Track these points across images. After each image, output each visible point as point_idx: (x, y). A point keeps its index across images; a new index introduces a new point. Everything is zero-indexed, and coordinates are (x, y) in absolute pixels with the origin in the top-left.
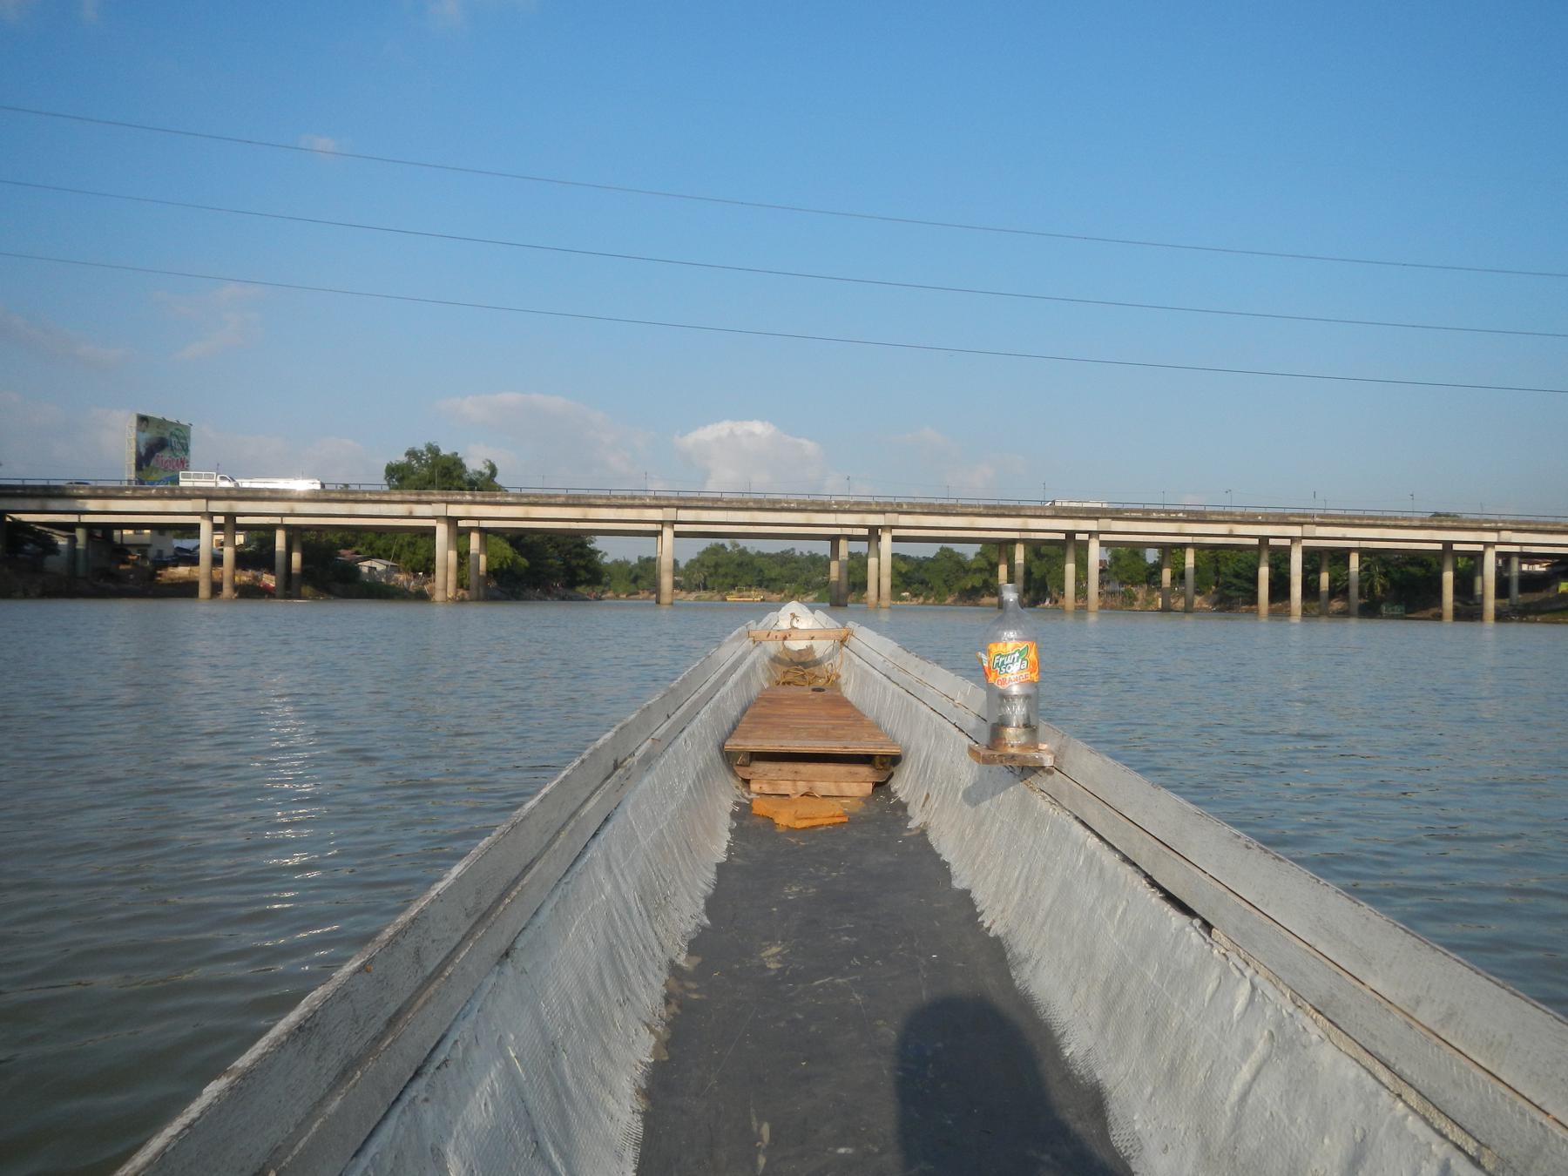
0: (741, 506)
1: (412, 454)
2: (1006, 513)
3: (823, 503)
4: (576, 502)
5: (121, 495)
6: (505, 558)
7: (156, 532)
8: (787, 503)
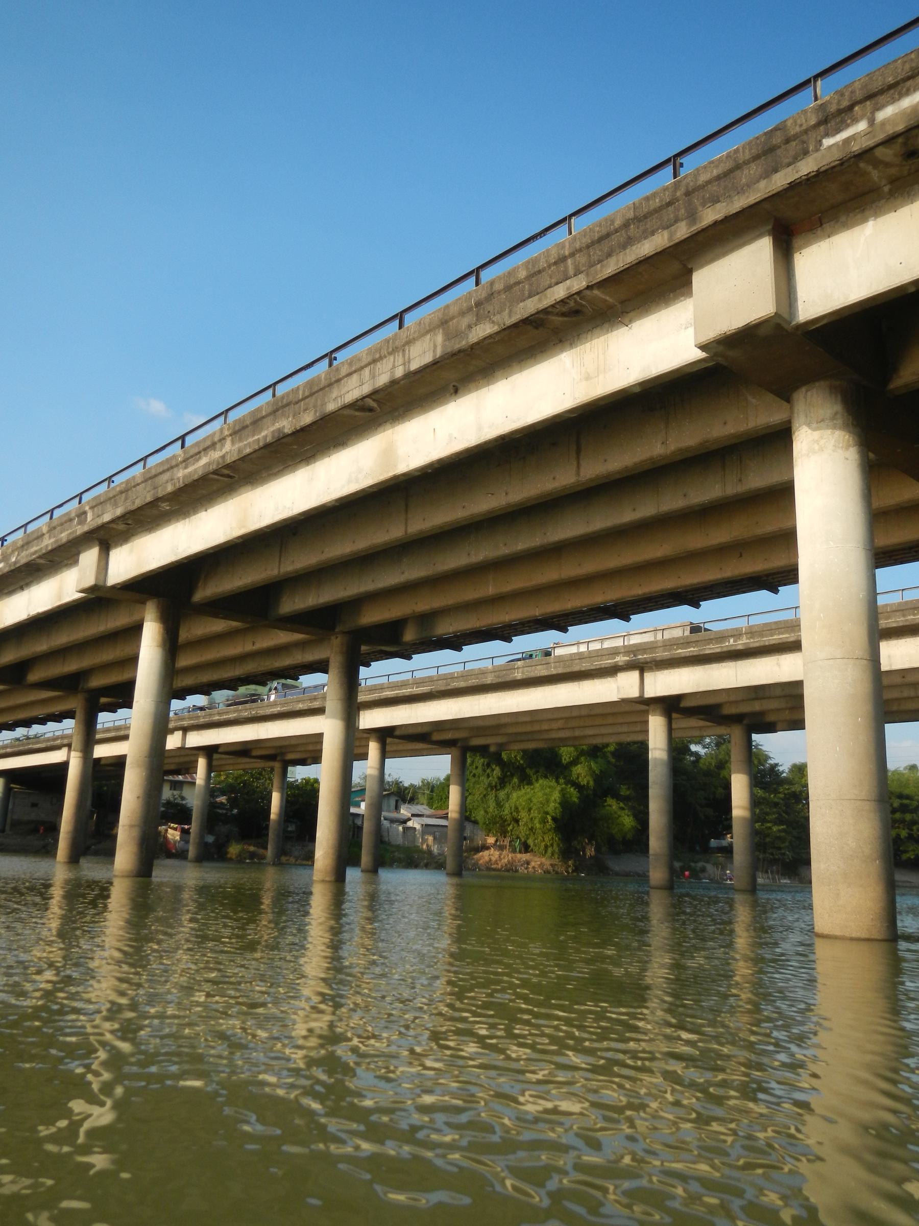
6: (547, 813)
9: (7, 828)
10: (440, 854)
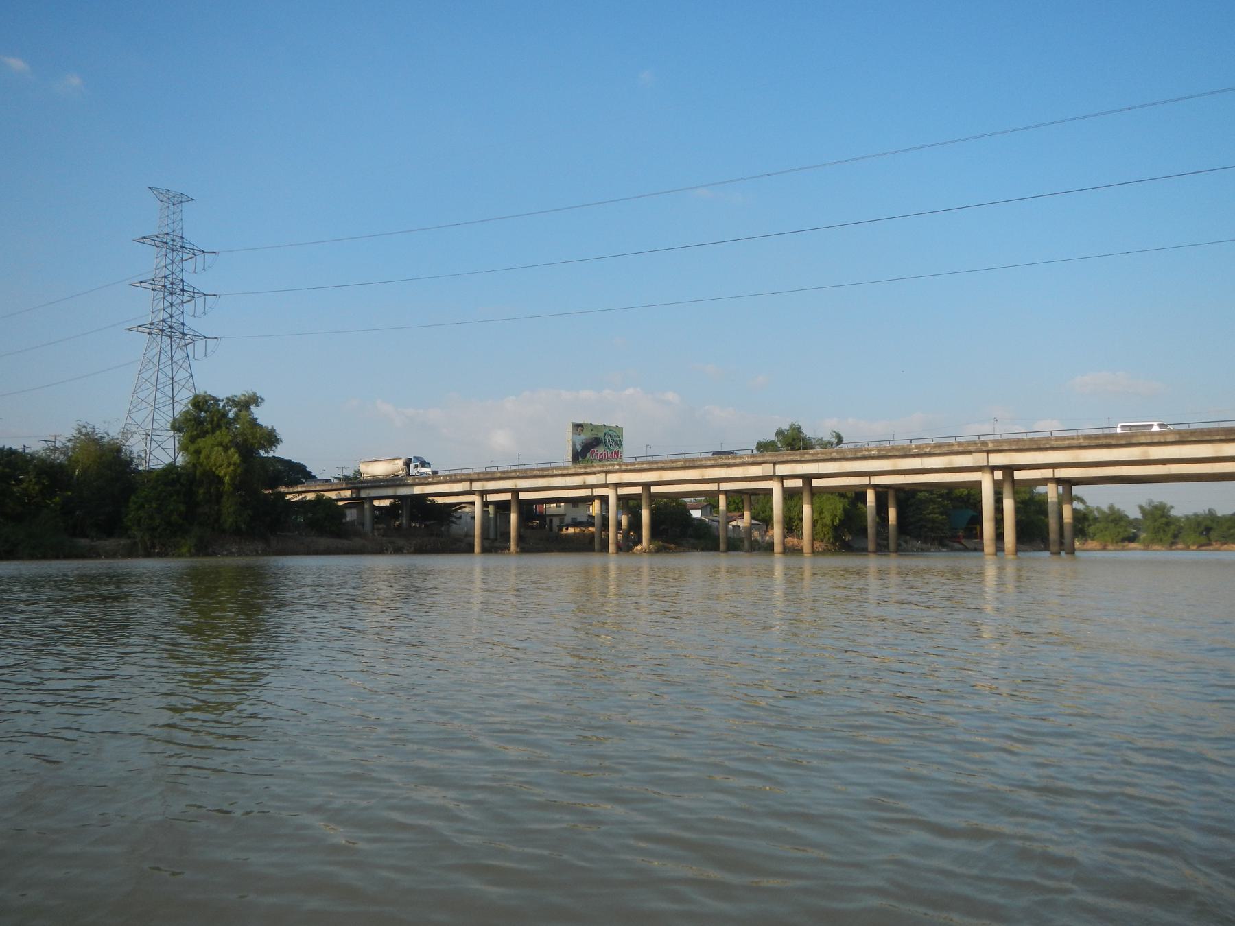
0: (826, 458)
1: (779, 433)
2: (1113, 442)
3: (903, 448)
4: (691, 465)
5: (426, 482)
6: (836, 516)
7: (570, 505)
8: (867, 450)
9: (498, 537)
10: (763, 542)
